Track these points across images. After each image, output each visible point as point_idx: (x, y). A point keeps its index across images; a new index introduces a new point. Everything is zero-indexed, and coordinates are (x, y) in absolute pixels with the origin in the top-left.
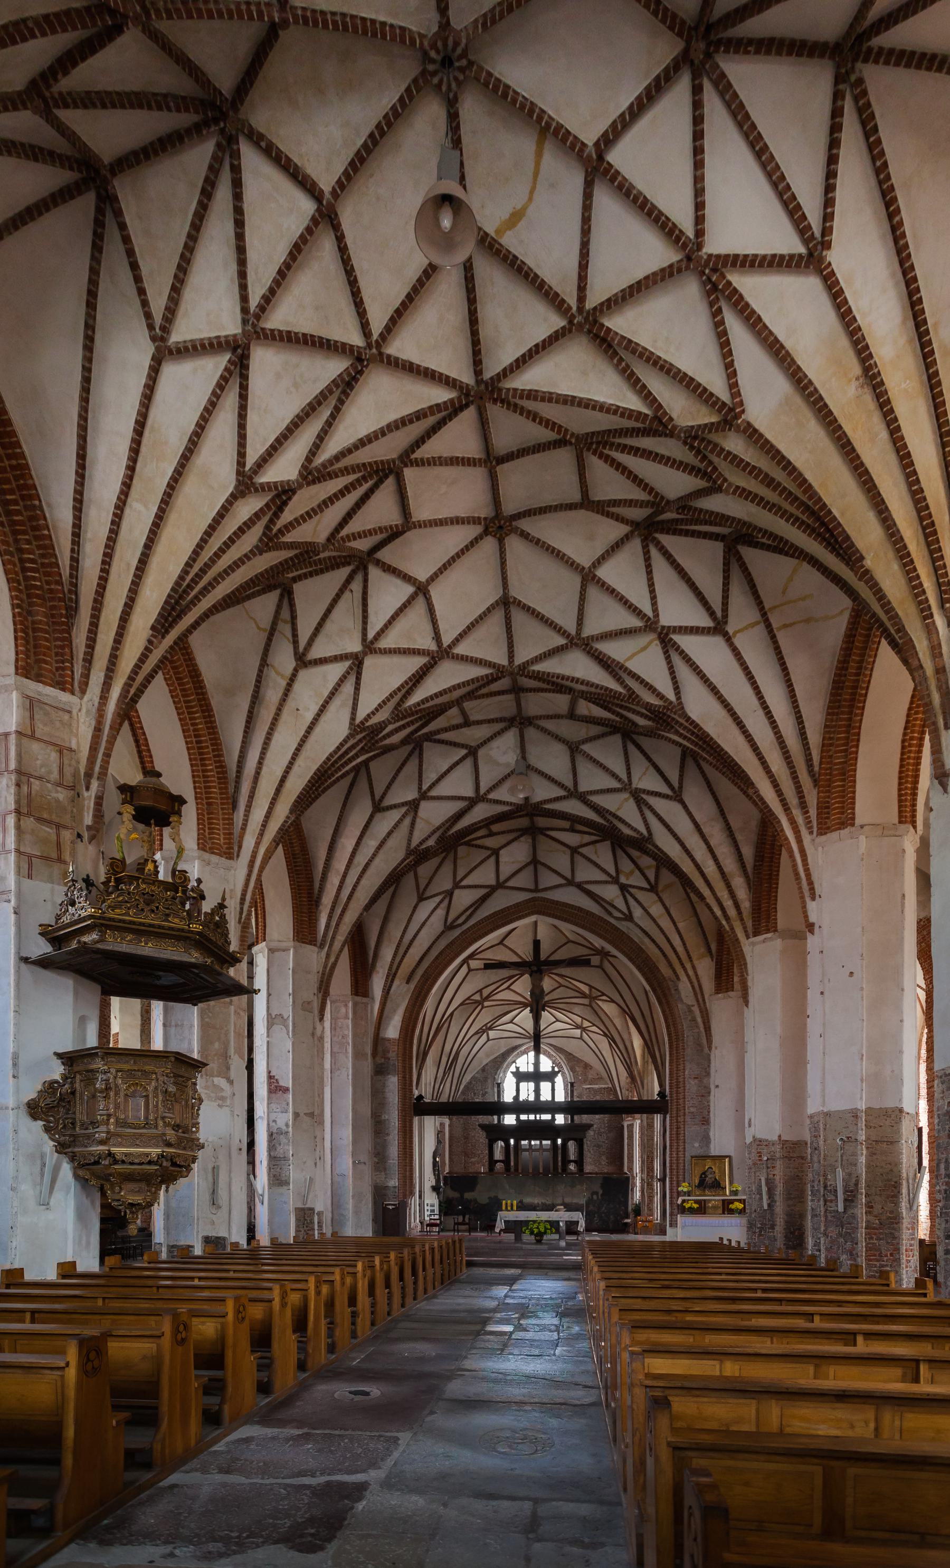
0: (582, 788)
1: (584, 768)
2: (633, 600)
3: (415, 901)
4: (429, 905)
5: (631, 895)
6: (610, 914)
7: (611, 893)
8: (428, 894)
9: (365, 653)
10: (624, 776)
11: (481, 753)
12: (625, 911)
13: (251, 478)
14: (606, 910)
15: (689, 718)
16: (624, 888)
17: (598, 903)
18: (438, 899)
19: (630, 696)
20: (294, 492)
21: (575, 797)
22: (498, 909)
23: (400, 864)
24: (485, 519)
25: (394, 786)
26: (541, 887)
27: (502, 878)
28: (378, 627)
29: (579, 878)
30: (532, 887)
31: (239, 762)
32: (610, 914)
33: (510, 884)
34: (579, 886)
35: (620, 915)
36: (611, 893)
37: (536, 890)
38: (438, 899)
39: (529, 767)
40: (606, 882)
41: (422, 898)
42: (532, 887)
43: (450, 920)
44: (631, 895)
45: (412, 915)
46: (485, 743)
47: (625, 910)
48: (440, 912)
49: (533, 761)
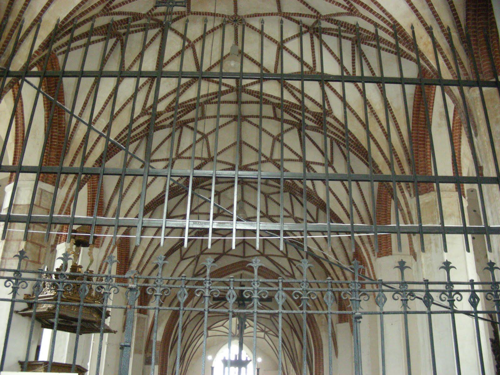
0: (270, 213)
1: (271, 204)
2: (294, 149)
3: (178, 259)
4: (186, 263)
5: (293, 263)
6: (283, 273)
7: (284, 262)
8: (185, 257)
9: (176, 159)
10: (290, 211)
11: (222, 194)
12: (291, 273)
13: (147, 111)
14: (281, 271)
15: (319, 197)
16: (290, 260)
17: (277, 266)
18: (191, 260)
19: (293, 184)
20: (162, 114)
21: (267, 217)
22: (223, 266)
23: (175, 245)
24: (234, 116)
25: (178, 207)
26: (246, 255)
27: (226, 251)
28: (184, 149)
29: (267, 252)
30: (242, 255)
31: (110, 200)
32: (283, 273)
33: (229, 253)
34: (267, 257)
35: (288, 274)
36: (284, 262)
37: (244, 257)
38: (191, 260)
39: (245, 201)
40: (281, 256)
41: (182, 259)
42: (242, 255)
43: (196, 271)
44: (293, 263)
45: (176, 268)
46: (224, 190)
47: (291, 273)
48: (192, 267)
49: (246, 198)
